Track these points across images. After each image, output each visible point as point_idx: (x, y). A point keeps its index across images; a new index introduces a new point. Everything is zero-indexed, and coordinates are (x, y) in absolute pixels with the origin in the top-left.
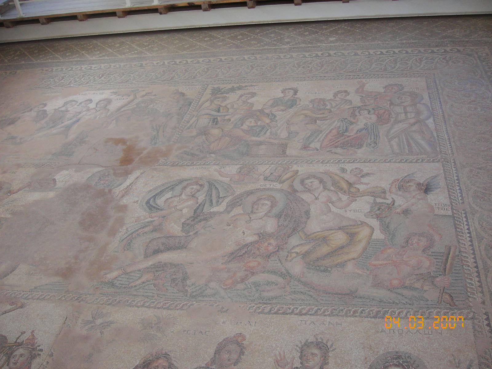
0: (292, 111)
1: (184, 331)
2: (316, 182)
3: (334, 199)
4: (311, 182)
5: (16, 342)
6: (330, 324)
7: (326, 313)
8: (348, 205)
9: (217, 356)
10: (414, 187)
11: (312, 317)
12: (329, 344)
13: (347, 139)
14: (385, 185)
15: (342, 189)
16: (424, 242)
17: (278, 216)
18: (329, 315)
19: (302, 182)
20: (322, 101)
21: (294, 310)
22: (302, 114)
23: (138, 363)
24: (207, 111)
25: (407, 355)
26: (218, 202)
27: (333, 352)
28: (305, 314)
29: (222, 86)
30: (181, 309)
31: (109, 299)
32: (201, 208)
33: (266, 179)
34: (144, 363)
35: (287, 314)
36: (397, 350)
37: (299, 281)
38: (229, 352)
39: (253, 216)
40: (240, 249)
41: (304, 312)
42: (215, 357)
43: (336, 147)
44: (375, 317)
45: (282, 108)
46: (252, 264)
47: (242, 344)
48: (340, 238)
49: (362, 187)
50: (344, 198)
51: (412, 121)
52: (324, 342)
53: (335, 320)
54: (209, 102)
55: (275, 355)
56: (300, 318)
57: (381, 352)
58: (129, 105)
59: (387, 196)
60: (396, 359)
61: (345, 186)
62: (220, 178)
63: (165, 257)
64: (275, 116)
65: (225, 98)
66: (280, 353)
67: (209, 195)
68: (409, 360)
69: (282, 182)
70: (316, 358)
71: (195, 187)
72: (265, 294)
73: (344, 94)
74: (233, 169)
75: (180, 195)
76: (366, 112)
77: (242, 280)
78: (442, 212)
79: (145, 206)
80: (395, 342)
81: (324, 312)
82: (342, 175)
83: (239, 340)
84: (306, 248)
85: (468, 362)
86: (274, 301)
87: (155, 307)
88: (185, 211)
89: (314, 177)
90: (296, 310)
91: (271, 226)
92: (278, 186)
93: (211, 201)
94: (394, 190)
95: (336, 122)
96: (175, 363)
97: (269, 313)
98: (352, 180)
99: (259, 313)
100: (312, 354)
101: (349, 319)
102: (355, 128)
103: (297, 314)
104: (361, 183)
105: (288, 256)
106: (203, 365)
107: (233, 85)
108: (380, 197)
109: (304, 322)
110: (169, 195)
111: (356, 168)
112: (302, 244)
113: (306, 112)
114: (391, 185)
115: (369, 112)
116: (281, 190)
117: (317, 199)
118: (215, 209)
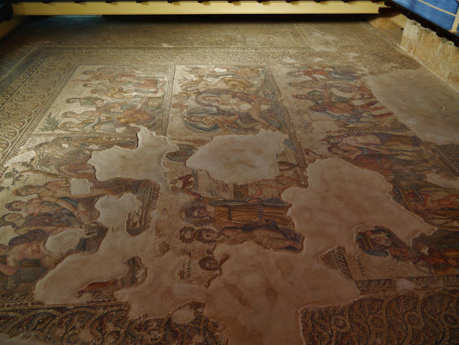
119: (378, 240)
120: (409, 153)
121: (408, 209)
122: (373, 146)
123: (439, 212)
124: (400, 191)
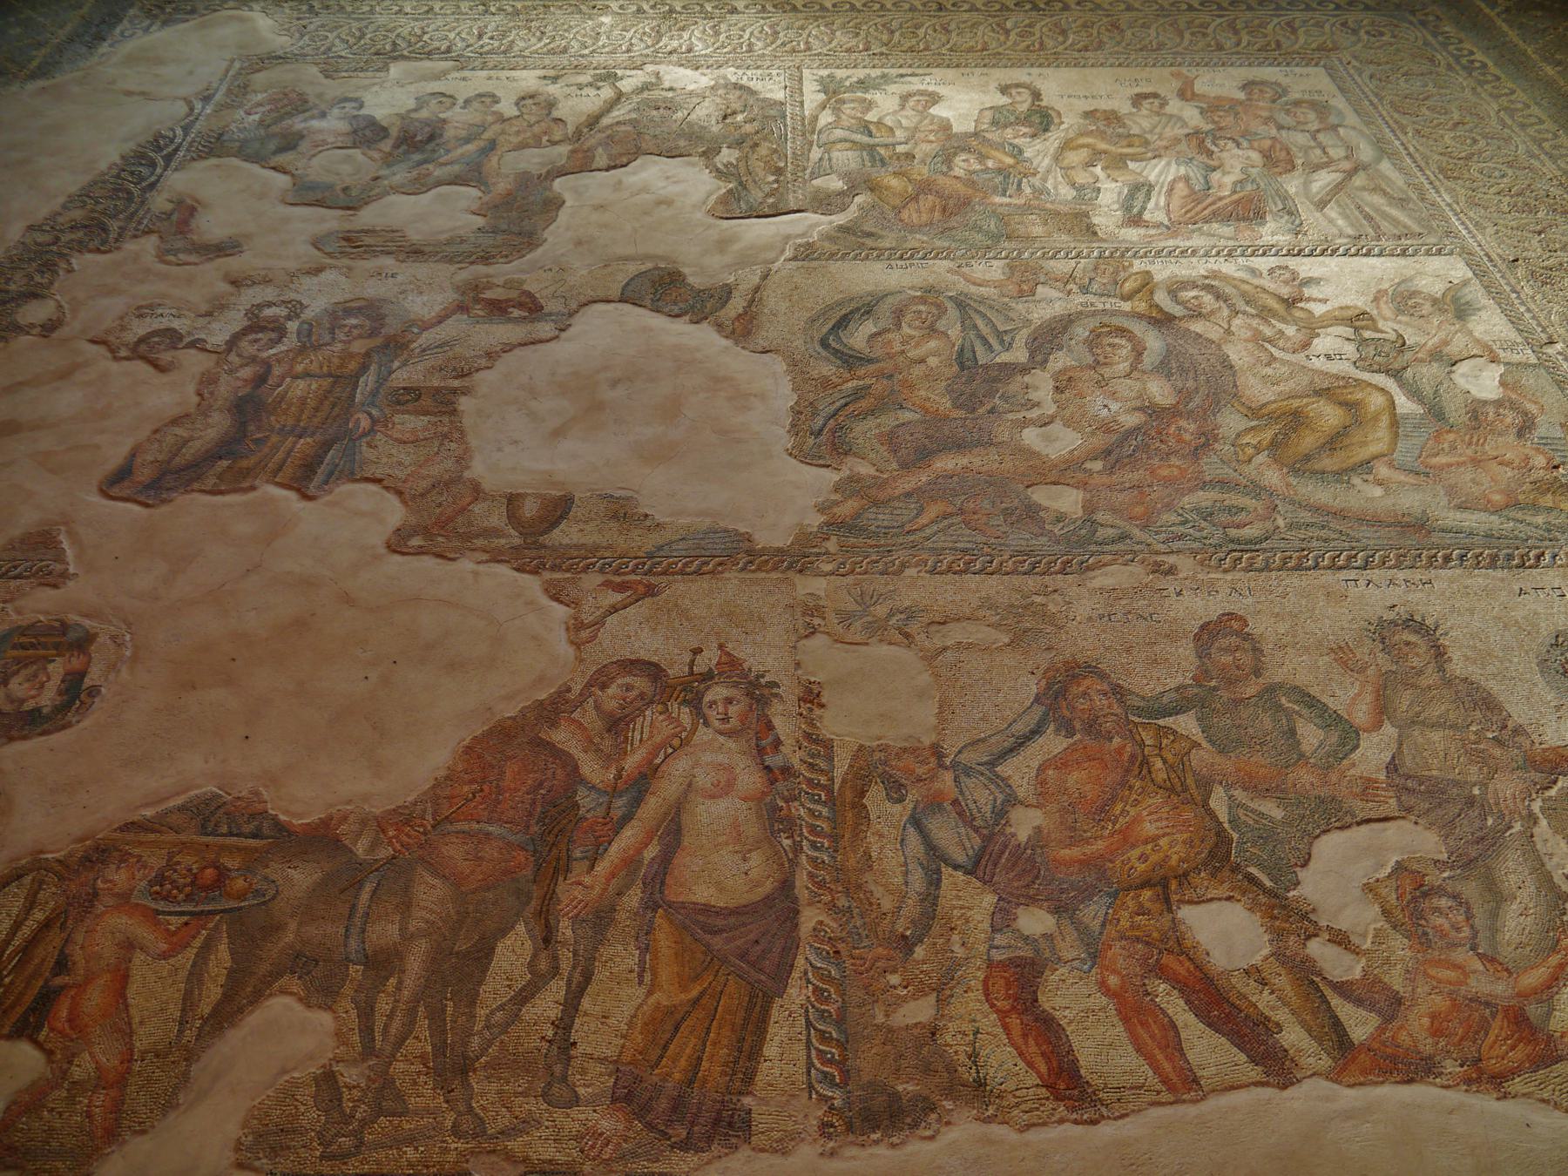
0: (1054, 139)
1: (1101, 617)
2: (1208, 299)
3: (1268, 332)
4: (1196, 297)
5: (691, 673)
8: (1306, 345)
10: (1427, 308)
13: (1220, 204)
14: (1361, 303)
15: (1274, 314)
16: (1510, 417)
17: (1163, 368)
19: (1173, 293)
20: (1112, 117)
22: (1087, 146)
23: (1034, 689)
24: (839, 133)
26: (1002, 342)
28: (1341, 568)
29: (840, 73)
30: (1063, 572)
32: (968, 354)
33: (1085, 290)
34: (1048, 687)
37: (1292, 502)
39: (1107, 372)
40: (1120, 444)
43: (1207, 221)
45: (1024, 130)
46: (1165, 472)
48: (1330, 416)
49: (1318, 309)
50: (1291, 331)
51: (1347, 165)
52: (1418, 618)
53: (1417, 575)
54: (828, 111)
56: (1344, 575)
58: (615, 113)
59: (1381, 324)
61: (1273, 303)
62: (973, 289)
63: (947, 463)
64: (1021, 152)
65: (869, 105)
67: (967, 324)
69: (1125, 298)
71: (922, 308)
72: (1233, 532)
73: (1157, 102)
74: (992, 270)
75: (899, 326)
76: (1230, 144)
77: (1169, 507)
78: (1516, 358)
79: (824, 353)
82: (1256, 281)
84: (1268, 435)
86: (1264, 545)
88: (933, 361)
89: (1195, 286)
91: (1159, 391)
92: (1126, 306)
93: (985, 342)
94: (1387, 310)
95: (1174, 166)
97: (1267, 568)
98: (1285, 291)
100: (1408, 644)
102: (1225, 182)
104: (1309, 300)
105: (1236, 453)
107: (867, 71)
108: (1366, 328)
110: (869, 327)
111: (1280, 267)
112: (1252, 428)
113: (1090, 140)
114: (1376, 299)
115: (1238, 145)
116: (1140, 316)
117: (1228, 332)
118: (1005, 357)
119: (35, 676)
120: (547, 1005)
121: (128, 827)
122: (651, 852)
123: (55, 938)
124: (252, 842)
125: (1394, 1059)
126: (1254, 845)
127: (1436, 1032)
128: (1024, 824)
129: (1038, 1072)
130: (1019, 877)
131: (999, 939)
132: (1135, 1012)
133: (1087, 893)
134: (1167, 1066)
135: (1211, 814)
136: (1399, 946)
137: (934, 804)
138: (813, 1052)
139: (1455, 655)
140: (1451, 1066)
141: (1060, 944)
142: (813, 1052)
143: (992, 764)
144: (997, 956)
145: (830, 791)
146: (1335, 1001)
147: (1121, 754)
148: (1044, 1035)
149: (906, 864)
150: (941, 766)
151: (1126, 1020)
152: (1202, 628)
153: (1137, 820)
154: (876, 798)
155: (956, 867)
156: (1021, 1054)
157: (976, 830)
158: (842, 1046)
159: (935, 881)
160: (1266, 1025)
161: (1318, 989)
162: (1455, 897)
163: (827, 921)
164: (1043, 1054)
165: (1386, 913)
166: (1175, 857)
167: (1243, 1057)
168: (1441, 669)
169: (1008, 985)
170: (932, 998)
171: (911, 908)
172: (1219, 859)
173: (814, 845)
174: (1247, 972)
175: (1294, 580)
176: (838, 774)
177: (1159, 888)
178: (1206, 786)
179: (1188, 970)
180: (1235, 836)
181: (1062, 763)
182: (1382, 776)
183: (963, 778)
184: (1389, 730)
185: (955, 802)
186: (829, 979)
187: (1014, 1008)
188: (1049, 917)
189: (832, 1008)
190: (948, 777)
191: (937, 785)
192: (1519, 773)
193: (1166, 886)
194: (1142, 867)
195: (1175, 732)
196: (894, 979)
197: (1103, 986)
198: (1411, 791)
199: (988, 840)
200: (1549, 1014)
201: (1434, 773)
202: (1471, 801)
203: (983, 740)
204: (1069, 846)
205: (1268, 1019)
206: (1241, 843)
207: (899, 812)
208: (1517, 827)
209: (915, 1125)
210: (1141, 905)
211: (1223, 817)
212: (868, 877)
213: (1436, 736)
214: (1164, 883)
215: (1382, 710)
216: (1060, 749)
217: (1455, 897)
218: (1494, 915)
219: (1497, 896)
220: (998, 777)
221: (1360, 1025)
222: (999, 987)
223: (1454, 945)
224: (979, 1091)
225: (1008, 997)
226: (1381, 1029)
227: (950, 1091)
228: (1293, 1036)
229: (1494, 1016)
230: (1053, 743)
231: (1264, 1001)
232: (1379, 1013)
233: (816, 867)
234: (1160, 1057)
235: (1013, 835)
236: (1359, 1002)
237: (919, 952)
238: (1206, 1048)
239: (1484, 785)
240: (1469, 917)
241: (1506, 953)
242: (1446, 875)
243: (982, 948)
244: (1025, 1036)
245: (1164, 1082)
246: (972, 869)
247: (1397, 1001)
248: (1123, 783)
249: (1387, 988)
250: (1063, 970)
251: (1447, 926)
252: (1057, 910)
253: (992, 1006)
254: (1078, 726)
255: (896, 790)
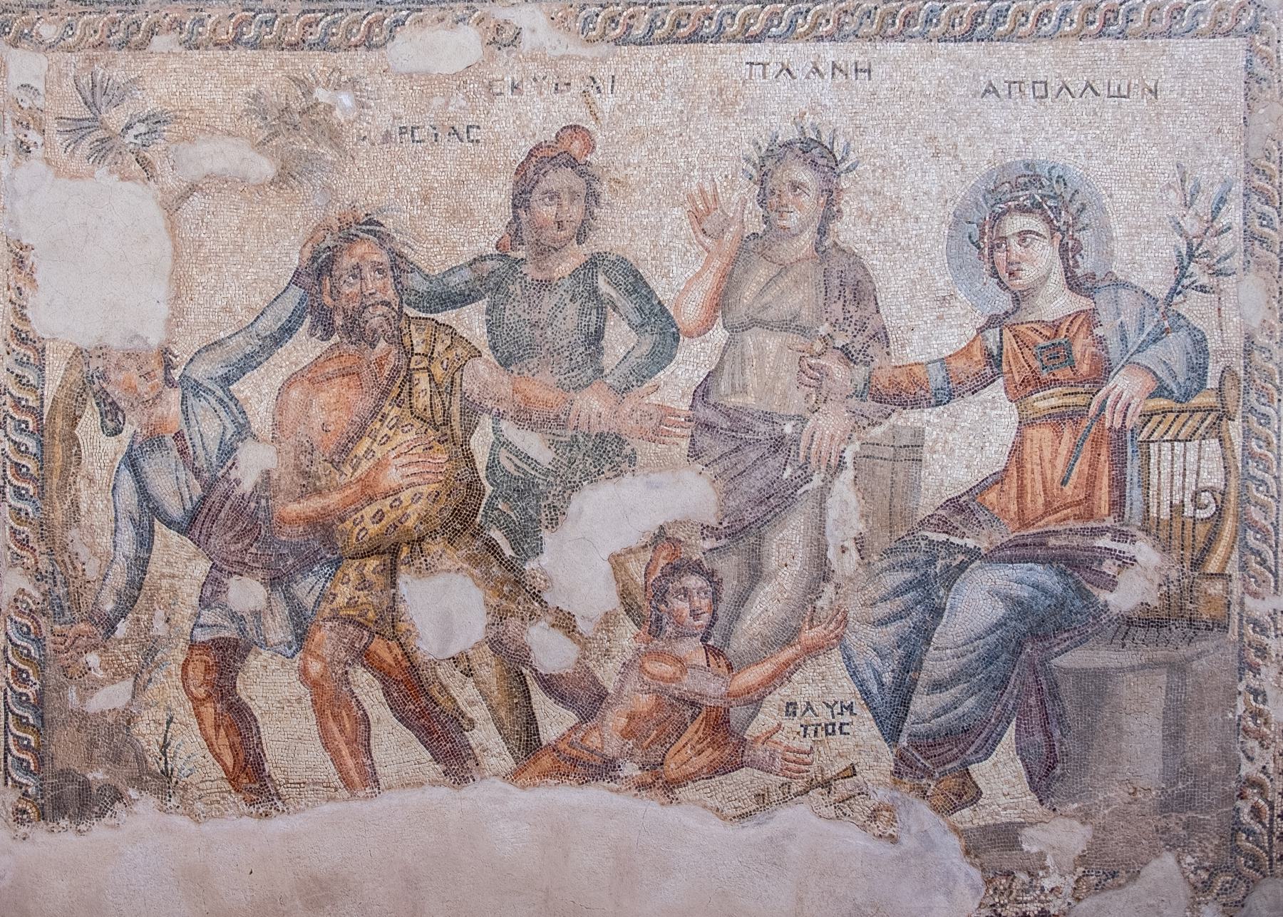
1: (403, 131)
6: (837, 72)
7: (823, 30)
9: (521, 212)
11: (782, 48)
12: (838, 150)
18: (831, 37)
21: (724, 24)
25: (1055, 174)
27: (850, 176)
31: (114, 22)
34: (314, 259)
35: (703, 40)
36: (1029, 157)
38: (553, 196)
41: (755, 29)
42: (516, 217)
44: (967, 37)
47: (587, 164)
52: (825, 139)
53: (848, 53)
55: (690, 197)
57: (985, 167)
60: (1025, 187)
66: (702, 191)
68: (1059, 189)
70: (804, 198)
80: (1024, 129)
81: (816, 25)
83: (576, 147)
85: (1217, 189)
87: (279, 45)
90: (729, 21)
96: (405, 250)
99: (616, 42)
100: (795, 186)
101: (895, 49)
103: (733, 39)
106: (491, 250)
109: (759, 69)
125: (574, 761)
126: (506, 499)
127: (627, 734)
128: (253, 463)
129: (224, 765)
130: (238, 538)
131: (207, 617)
132: (331, 703)
133: (307, 562)
134: (350, 763)
135: (469, 458)
136: (628, 636)
137: (154, 441)
138: (11, 738)
139: (848, 206)
140: (630, 769)
141: (269, 621)
142: (11, 738)
143: (227, 380)
144: (201, 636)
145: (37, 413)
146: (539, 698)
147: (381, 366)
148: (236, 721)
149: (116, 520)
150: (169, 382)
151: (320, 713)
152: (531, 154)
153: (380, 465)
154: (90, 421)
155: (169, 524)
156: (210, 745)
157: (197, 473)
158: (38, 733)
159: (145, 541)
160: (460, 721)
161: (524, 682)
162: (710, 576)
163: (29, 588)
164: (232, 746)
165: (625, 594)
166: (414, 517)
167: (427, 755)
168: (822, 232)
169: (208, 669)
170: (128, 684)
171: (119, 578)
172: (461, 517)
173: (19, 494)
174: (455, 660)
175: (679, 59)
176: (50, 391)
177: (387, 557)
178: (471, 412)
179: (395, 659)
180: (489, 489)
181: (312, 376)
182: (684, 406)
183: (191, 400)
184: (719, 335)
185: (178, 436)
186: (28, 658)
187: (209, 696)
188: (262, 588)
189: (31, 692)
190: (174, 396)
191: (159, 410)
192: (853, 402)
193: (393, 551)
194: (373, 529)
195: (454, 334)
196: (93, 659)
197: (304, 672)
198: (718, 428)
199: (209, 487)
200: (753, 716)
201: (750, 400)
202: (778, 444)
203: (219, 343)
204: (297, 500)
205: (463, 715)
206: (493, 497)
207: (114, 447)
208: (817, 481)
209: (101, 815)
210: (363, 578)
211: (481, 461)
212: (74, 533)
213: (773, 342)
214: (395, 551)
215: (721, 301)
216: (313, 356)
217: (710, 576)
218: (742, 600)
219: (755, 574)
220: (232, 398)
221: (554, 721)
222: (196, 672)
223: (681, 636)
224: (164, 782)
225: (205, 682)
226: (574, 729)
227: (138, 782)
228: (485, 737)
229: (693, 718)
230: (304, 348)
231: (465, 694)
232: (579, 714)
233: (18, 519)
234: (345, 752)
235: (238, 482)
236: (561, 698)
237: (122, 628)
238: (395, 745)
239: (802, 420)
240: (716, 599)
241: (739, 644)
242: (708, 544)
243: (187, 627)
244: (217, 727)
245: (343, 779)
246: (189, 525)
247: (602, 696)
248: (376, 413)
249: (595, 681)
250: (266, 654)
251: (687, 612)
252: (274, 582)
253: (188, 691)
254: (339, 321)
255: (112, 416)
